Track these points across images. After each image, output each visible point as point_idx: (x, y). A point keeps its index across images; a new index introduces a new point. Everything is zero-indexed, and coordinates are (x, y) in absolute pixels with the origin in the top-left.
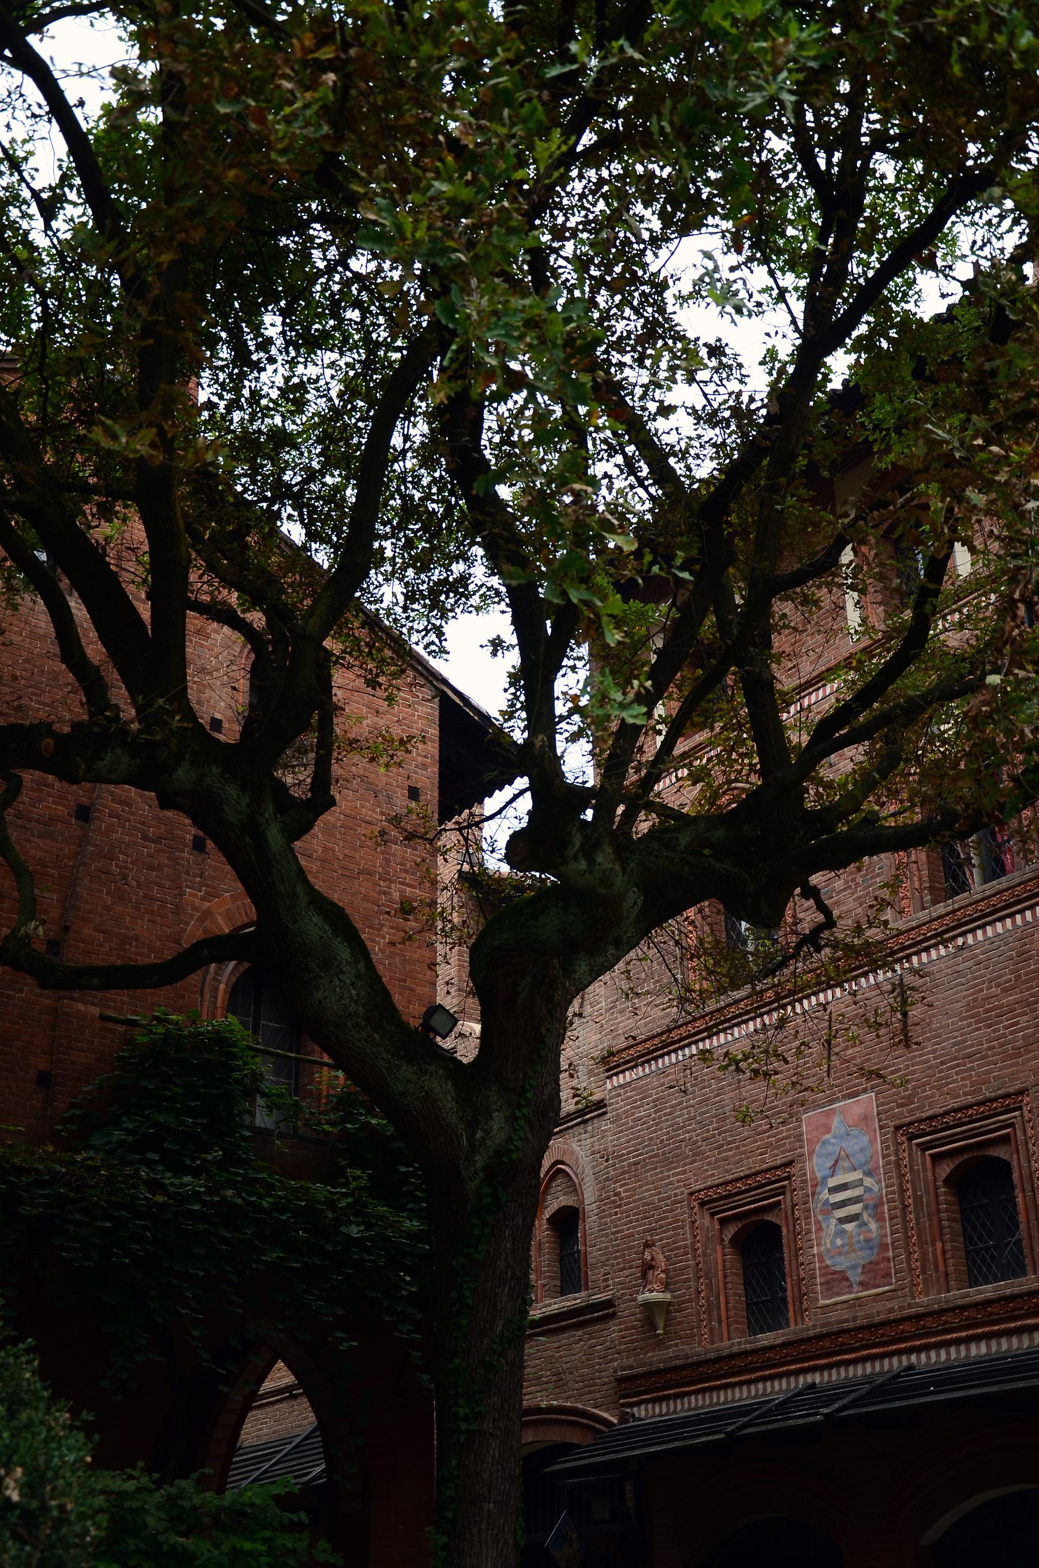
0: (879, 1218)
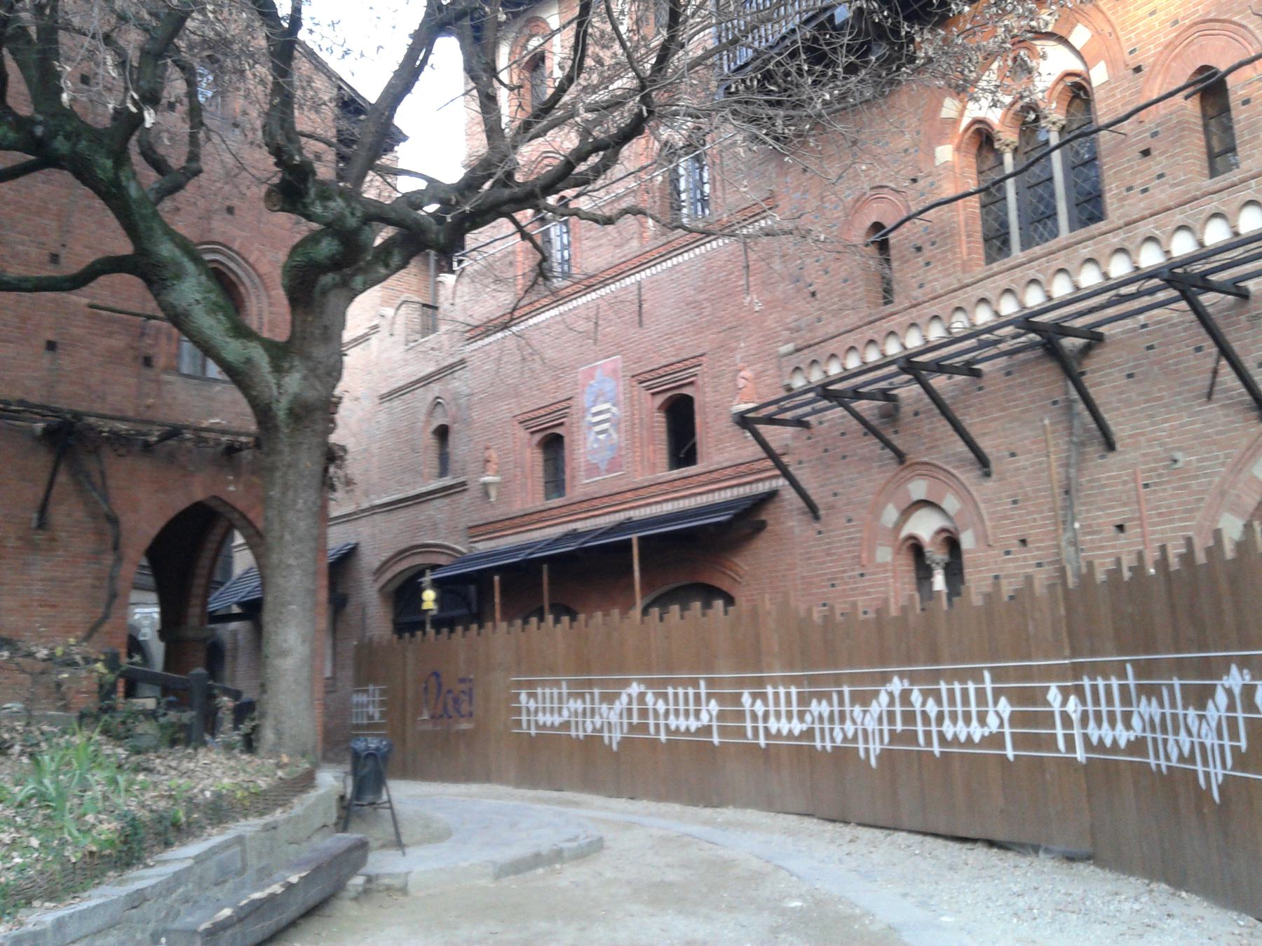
0: (618, 431)
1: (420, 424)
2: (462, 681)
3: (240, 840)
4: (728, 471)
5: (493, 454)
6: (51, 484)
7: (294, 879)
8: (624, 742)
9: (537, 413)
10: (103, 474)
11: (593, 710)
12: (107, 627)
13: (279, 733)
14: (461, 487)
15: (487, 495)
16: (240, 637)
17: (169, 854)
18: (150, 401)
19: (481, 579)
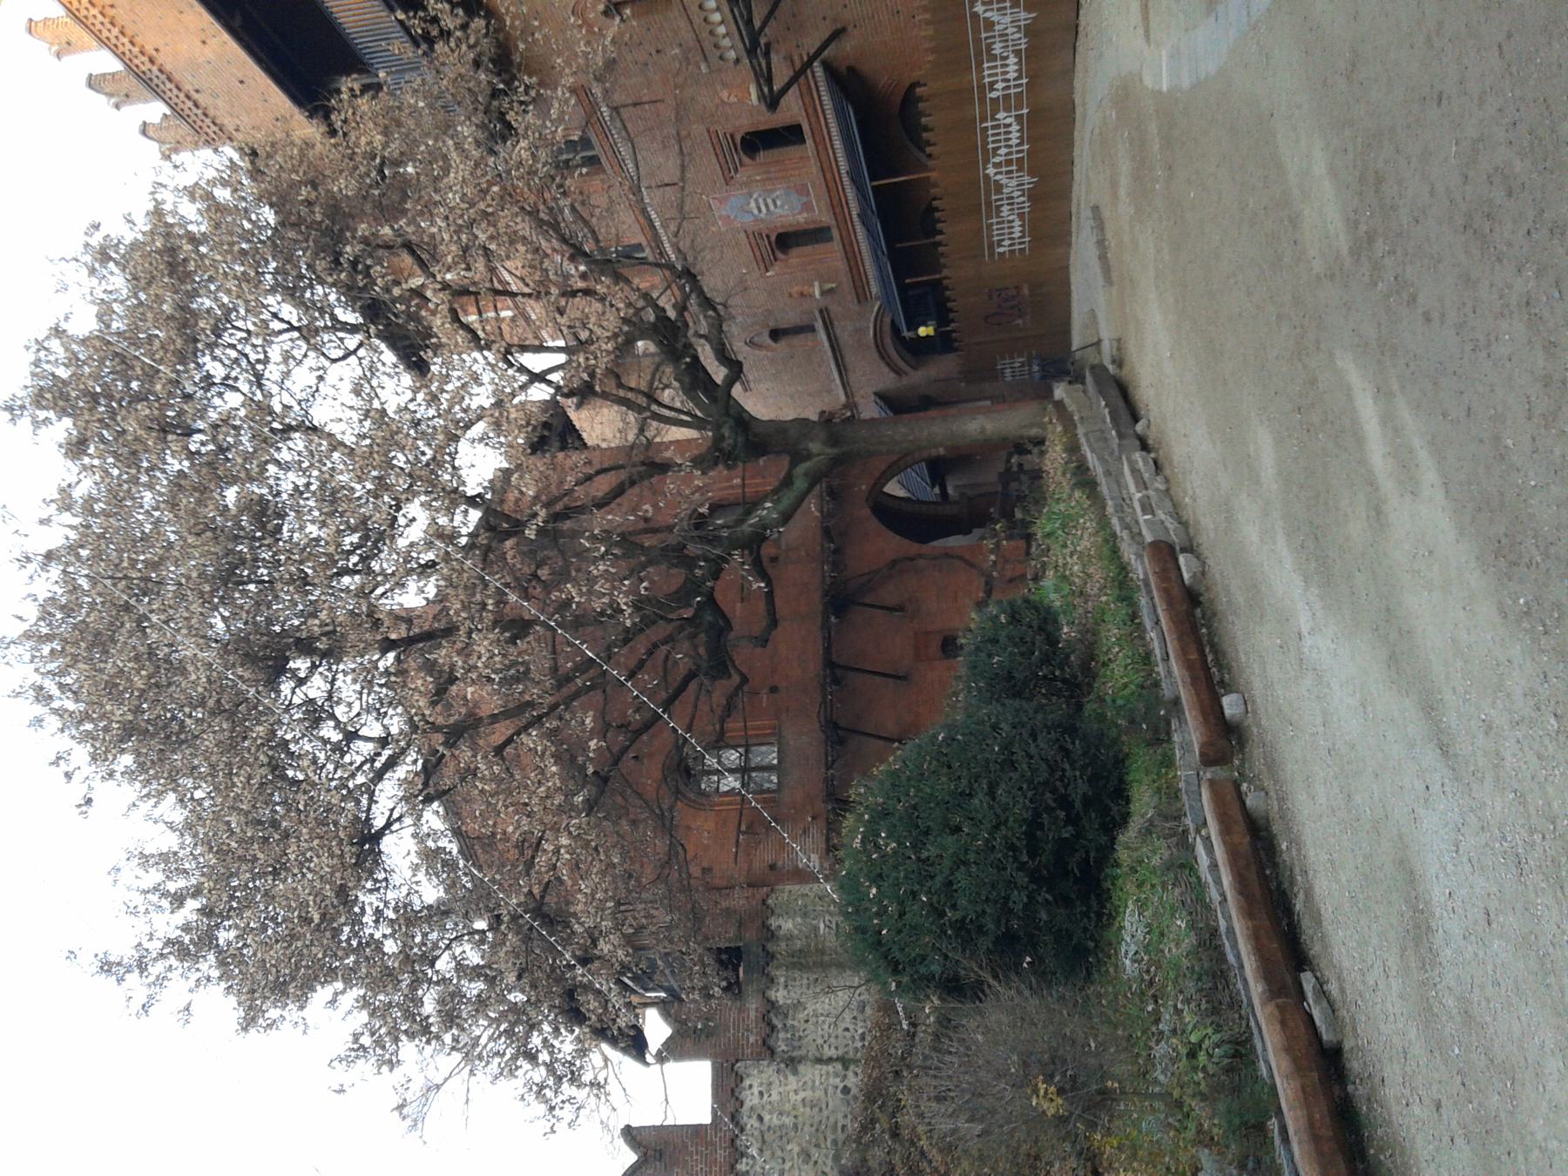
1: (769, 354)
2: (990, 297)
3: (1086, 435)
4: (807, 100)
5: (795, 290)
6: (873, 606)
7: (1103, 403)
8: (1031, 173)
9: (759, 258)
11: (1008, 198)
12: (967, 557)
13: (1032, 425)
14: (825, 313)
15: (831, 290)
16: (960, 483)
17: (1091, 466)
18: (803, 553)
19: (902, 289)
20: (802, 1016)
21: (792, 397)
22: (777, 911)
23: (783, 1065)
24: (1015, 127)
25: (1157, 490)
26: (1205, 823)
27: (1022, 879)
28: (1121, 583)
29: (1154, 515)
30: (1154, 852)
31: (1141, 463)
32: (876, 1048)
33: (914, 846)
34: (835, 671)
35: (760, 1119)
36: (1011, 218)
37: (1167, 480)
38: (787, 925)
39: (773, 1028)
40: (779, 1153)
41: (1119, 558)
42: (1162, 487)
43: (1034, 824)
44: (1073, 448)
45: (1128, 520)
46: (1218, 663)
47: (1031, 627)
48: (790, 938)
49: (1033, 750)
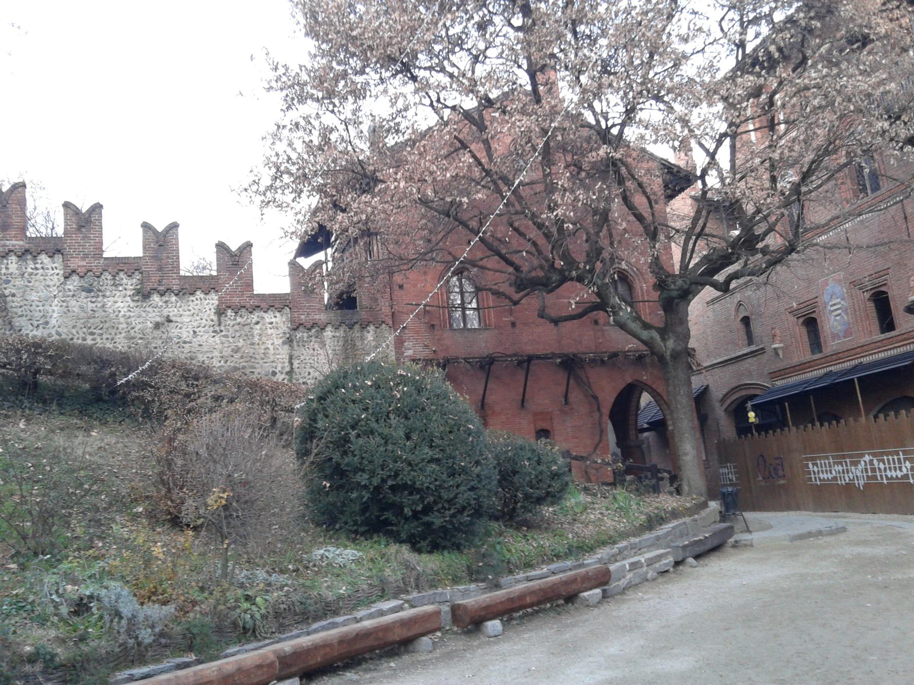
0: (847, 314)
2: (777, 459)
3: (685, 523)
7: (707, 535)
8: (865, 485)
10: (587, 377)
12: (601, 445)
13: (689, 486)
14: (762, 351)
15: (777, 354)
19: (780, 401)
20: (316, 346)
21: (704, 333)
22: (378, 330)
23: (288, 336)
24: (899, 474)
25: (647, 573)
26: (412, 606)
27: (376, 481)
28: (581, 547)
29: (630, 570)
30: (394, 571)
31: (665, 562)
32: (284, 389)
33: (397, 409)
34: (526, 362)
35: (257, 323)
36: (833, 472)
37: (654, 580)
38: (370, 336)
39: (309, 329)
40: (238, 334)
41: (599, 546)
42: (649, 576)
43: (412, 489)
44: (675, 514)
45: (626, 552)
46: (526, 615)
47: (549, 486)
48: (362, 338)
49: (462, 488)
